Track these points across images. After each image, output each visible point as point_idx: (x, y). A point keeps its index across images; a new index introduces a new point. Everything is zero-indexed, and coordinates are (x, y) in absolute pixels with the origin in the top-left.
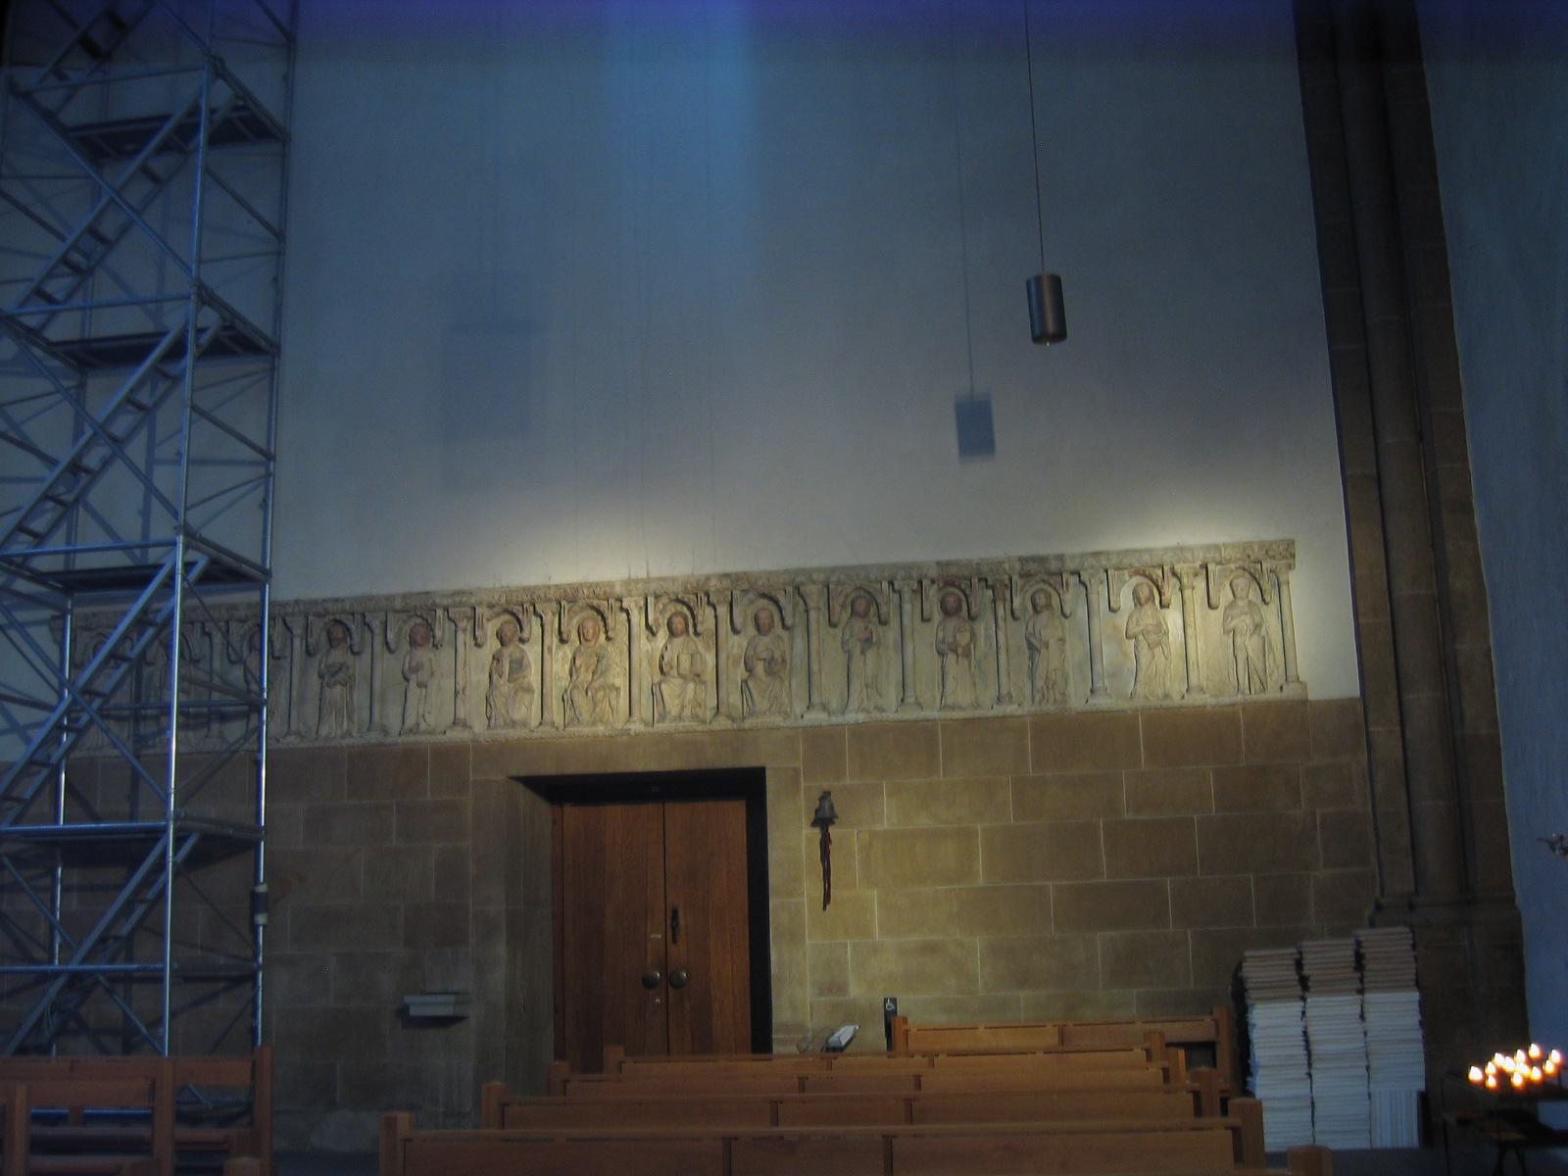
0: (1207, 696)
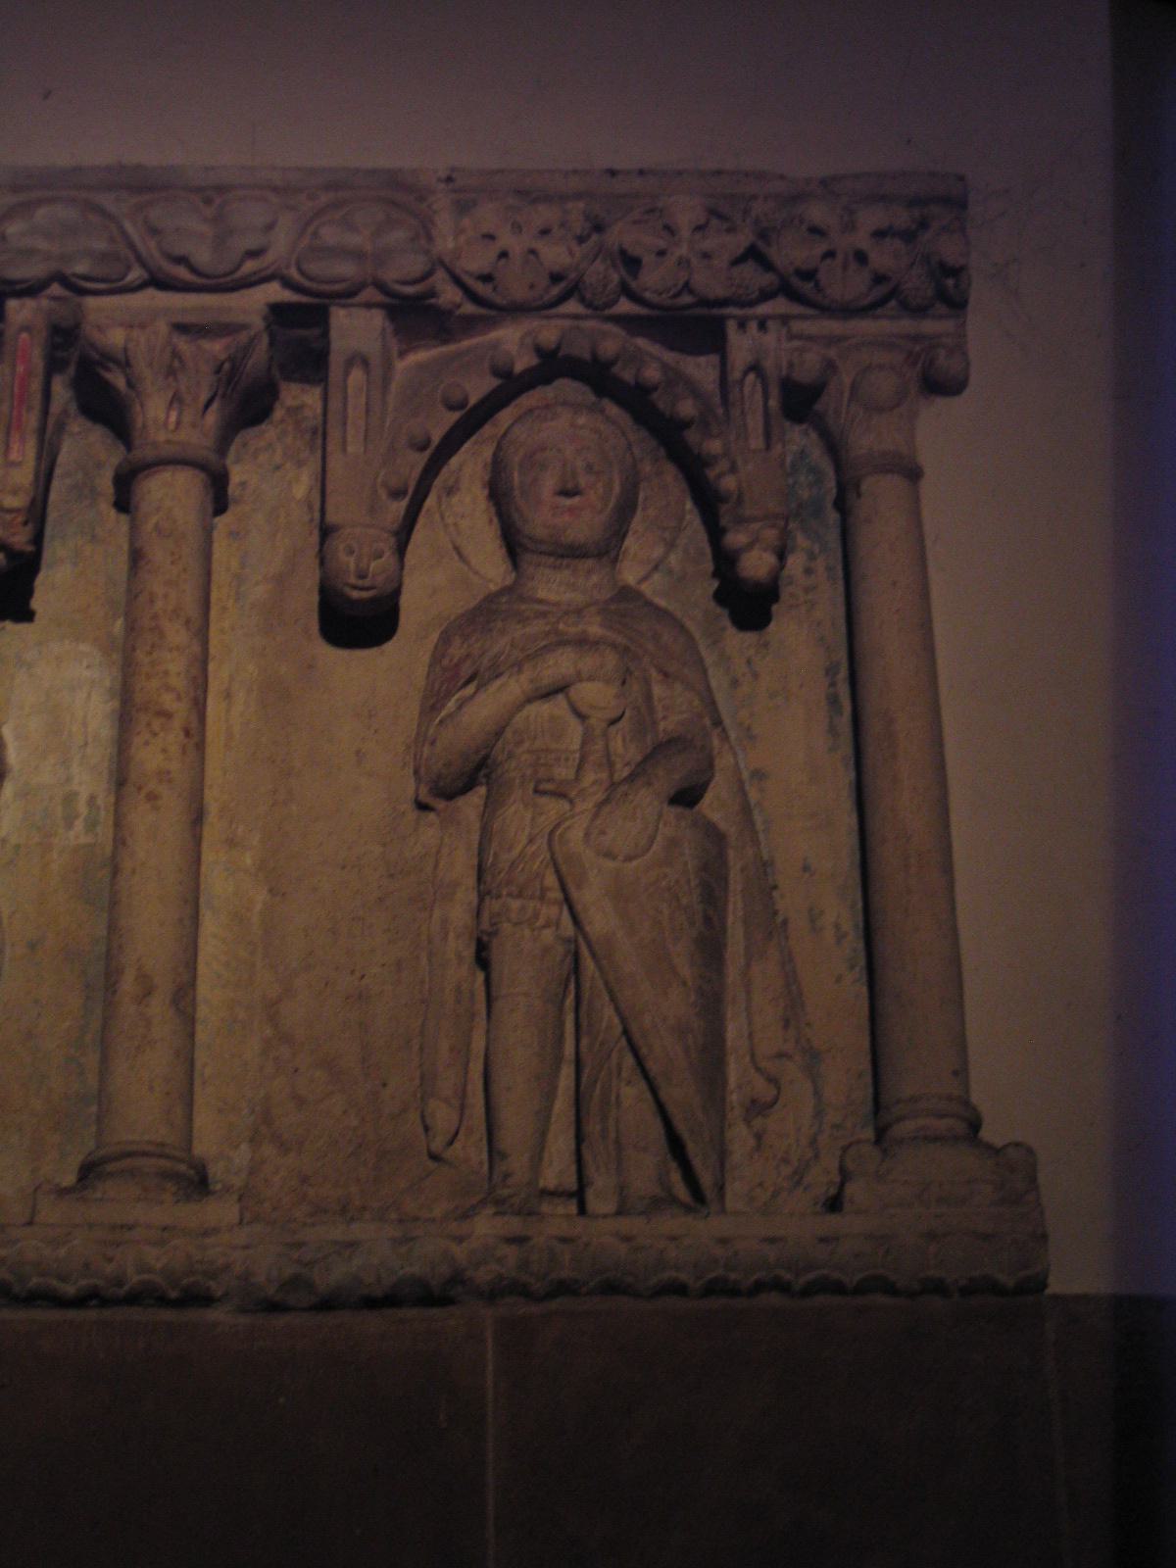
0: (220, 1211)
